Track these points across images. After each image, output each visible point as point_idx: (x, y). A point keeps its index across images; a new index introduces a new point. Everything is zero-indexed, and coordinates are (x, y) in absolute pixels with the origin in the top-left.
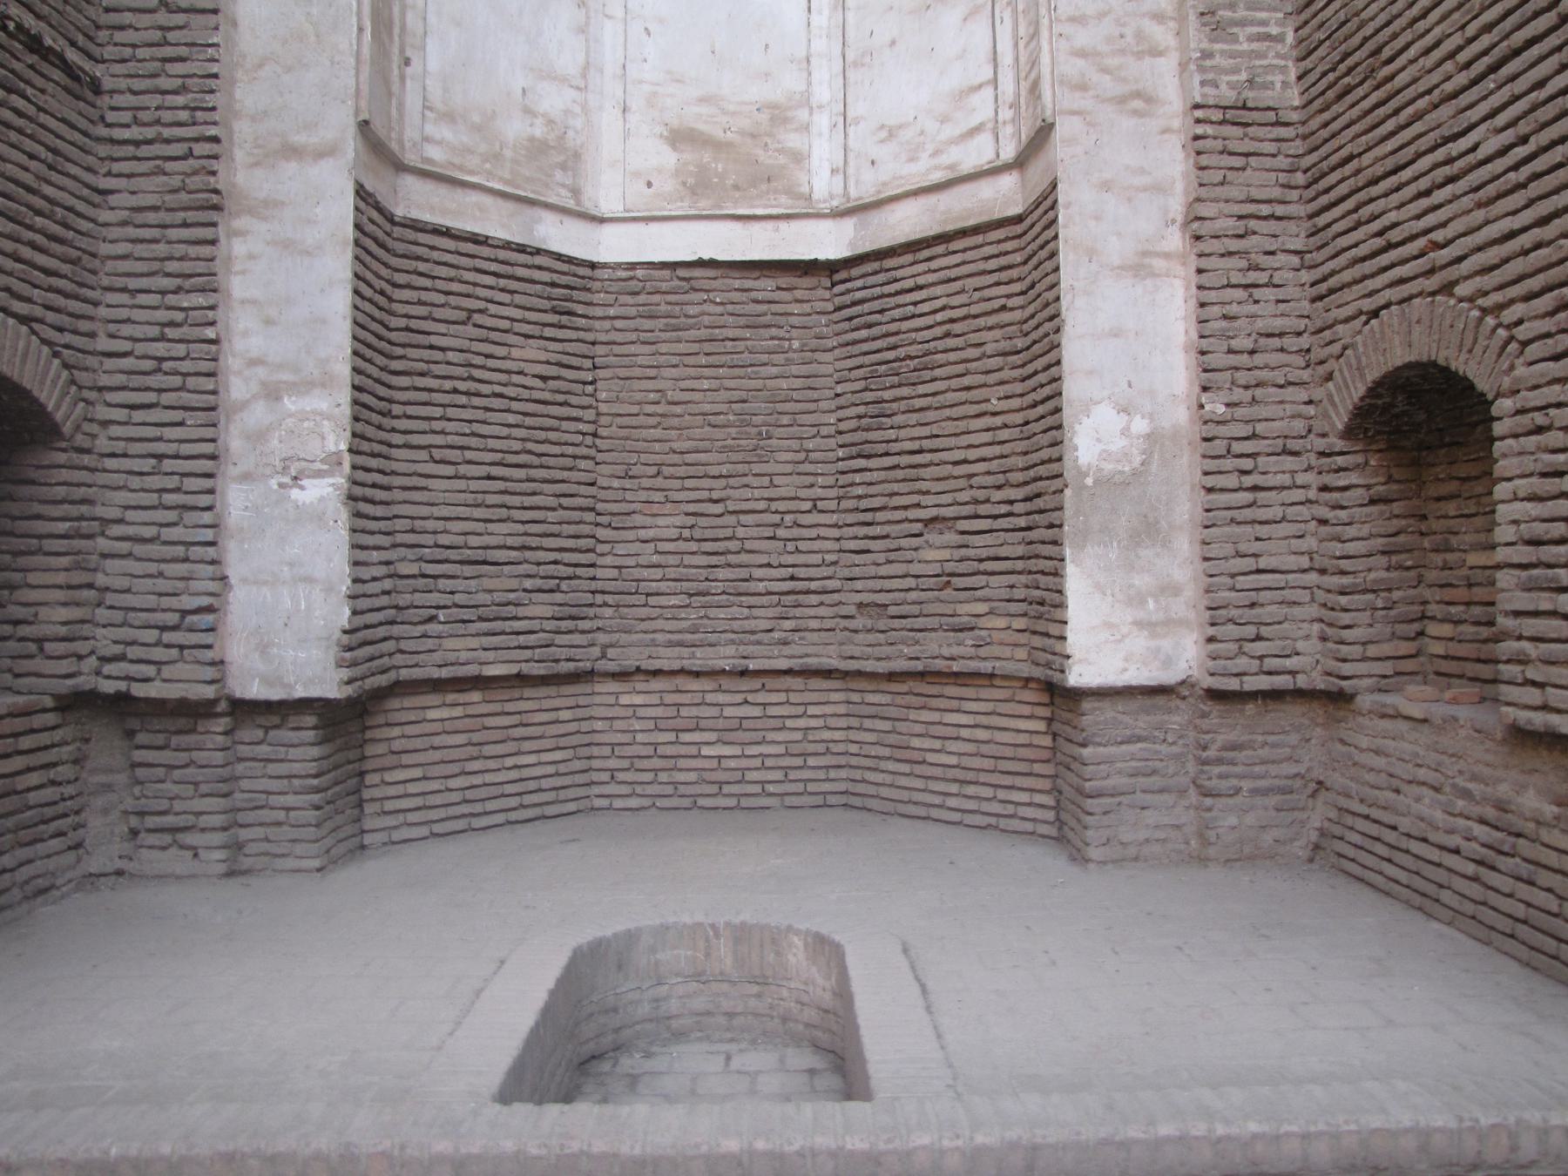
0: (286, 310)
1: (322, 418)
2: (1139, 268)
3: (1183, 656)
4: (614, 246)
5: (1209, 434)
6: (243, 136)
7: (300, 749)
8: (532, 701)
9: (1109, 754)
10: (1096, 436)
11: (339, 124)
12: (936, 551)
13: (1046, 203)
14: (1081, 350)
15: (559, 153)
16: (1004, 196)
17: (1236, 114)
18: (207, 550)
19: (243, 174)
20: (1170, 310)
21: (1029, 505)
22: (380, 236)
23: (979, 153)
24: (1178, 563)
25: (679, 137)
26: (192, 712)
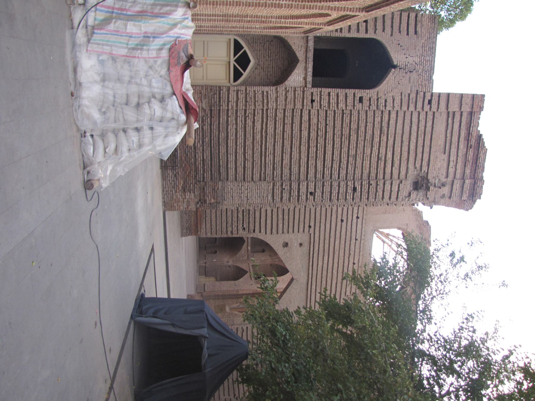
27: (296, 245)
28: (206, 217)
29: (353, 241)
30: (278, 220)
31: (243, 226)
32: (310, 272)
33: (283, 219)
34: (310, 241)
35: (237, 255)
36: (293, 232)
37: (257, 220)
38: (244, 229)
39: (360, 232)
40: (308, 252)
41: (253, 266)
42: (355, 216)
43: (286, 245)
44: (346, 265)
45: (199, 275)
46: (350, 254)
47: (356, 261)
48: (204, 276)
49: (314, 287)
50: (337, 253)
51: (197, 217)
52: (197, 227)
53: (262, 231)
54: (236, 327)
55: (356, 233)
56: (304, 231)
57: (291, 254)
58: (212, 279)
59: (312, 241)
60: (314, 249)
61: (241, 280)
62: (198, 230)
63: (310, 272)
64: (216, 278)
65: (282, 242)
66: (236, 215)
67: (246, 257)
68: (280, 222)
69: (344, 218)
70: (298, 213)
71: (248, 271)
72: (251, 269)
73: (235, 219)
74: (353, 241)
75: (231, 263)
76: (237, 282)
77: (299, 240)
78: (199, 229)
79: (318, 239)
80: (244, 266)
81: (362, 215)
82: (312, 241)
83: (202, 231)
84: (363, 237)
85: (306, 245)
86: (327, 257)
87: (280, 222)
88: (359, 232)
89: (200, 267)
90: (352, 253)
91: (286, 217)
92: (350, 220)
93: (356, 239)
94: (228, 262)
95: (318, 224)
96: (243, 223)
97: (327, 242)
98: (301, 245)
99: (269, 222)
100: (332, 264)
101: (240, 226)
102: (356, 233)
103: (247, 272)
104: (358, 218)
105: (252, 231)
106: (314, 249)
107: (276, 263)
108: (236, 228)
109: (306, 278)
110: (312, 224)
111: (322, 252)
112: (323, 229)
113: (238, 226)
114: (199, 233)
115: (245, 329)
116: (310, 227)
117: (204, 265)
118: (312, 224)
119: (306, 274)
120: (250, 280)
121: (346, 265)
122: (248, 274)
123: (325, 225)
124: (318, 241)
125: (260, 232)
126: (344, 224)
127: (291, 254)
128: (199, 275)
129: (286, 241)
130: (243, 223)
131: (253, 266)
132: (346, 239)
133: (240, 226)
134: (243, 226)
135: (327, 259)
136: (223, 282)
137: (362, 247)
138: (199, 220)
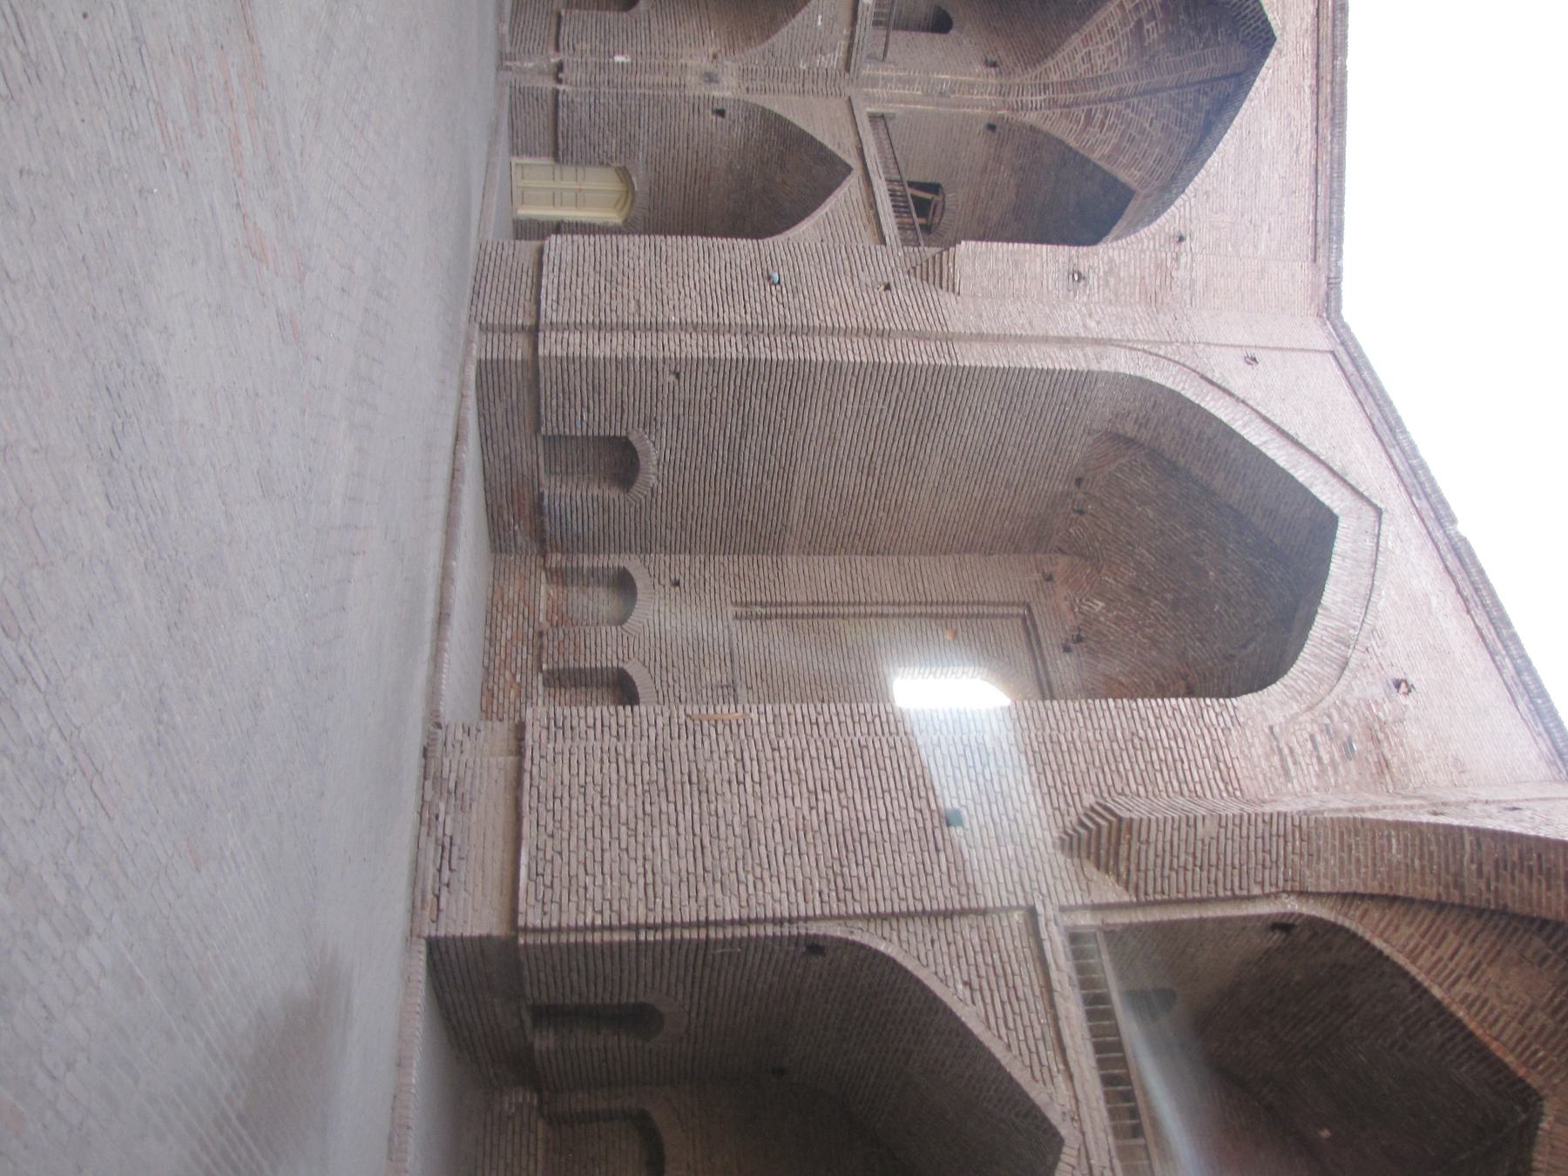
35: (781, 39)
41: (873, 118)
45: (515, 150)
48: (547, 161)
58: (602, 182)
61: (805, 231)
64: (624, 175)
67: (834, 59)
71: (853, 161)
72: (871, 151)
75: (728, 89)
76: (775, 245)
80: (821, 121)
89: (520, 99)
94: (710, 78)
103: (849, 169)
107: (1031, 118)
117: (549, 84)
120: (868, 238)
122: (850, 188)
128: (515, 150)
131: (873, 118)
136: (672, 244)
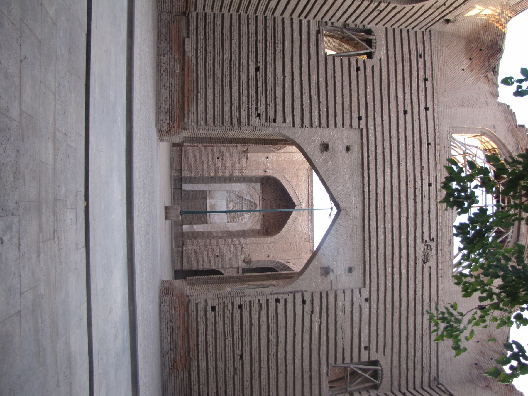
0: (201, 187)
1: (196, 189)
2: (203, 229)
3: (184, 231)
4: (208, 201)
5: (194, 232)
6: (210, 184)
7: (179, 187)
8: (180, 197)
9: (179, 227)
10: (195, 226)
11: (210, 189)
12: (189, 220)
13: (207, 223)
14: (199, 225)
15: (213, 198)
16: (209, 222)
17: (211, 233)
18: (189, 183)
19: (208, 184)
20: (201, 230)
21: (192, 223)
22: (205, 191)
23: (211, 221)
24: (189, 231)
25: (214, 204)
26: (181, 182)
27: (341, 148)
28: (197, 92)
29: (425, 146)
30: (311, 105)
31: (257, 109)
32: (366, 195)
33: (319, 102)
34: (362, 143)
36: (336, 126)
37: (279, 101)
38: (259, 115)
39: (433, 132)
40: (360, 162)
42: (423, 106)
43: (325, 147)
44: (418, 186)
46: (422, 167)
47: (432, 180)
49: (373, 223)
50: (403, 164)
51: (183, 94)
52: (182, 109)
53: (288, 120)
54: (248, 299)
55: (427, 133)
56: (351, 125)
57: (334, 164)
59: (365, 142)
60: (368, 157)
62: (184, 114)
63: (366, 195)
65: (318, 141)
66: (245, 92)
68: (315, 106)
69: (408, 108)
70: (340, 94)
73: (245, 99)
74: (425, 146)
77: (345, 141)
78: (186, 112)
79: (373, 139)
81: (432, 105)
82: (365, 142)
83: (191, 116)
84: (437, 141)
85: (356, 148)
86: (389, 171)
87: (315, 106)
88: (431, 131)
90: (425, 165)
91: (323, 100)
92: (416, 111)
93: (429, 144)
95: (371, 114)
96: (257, 105)
97: (387, 144)
98: (348, 149)
99: (297, 105)
100: (397, 183)
101: (253, 111)
102: (427, 133)
104: (427, 109)
105: (272, 120)
106: (368, 157)
108: (245, 114)
109: (360, 206)
110: (363, 114)
111: (382, 163)
112: (380, 123)
113: (248, 108)
114: (186, 120)
115: (264, 305)
116: (360, 118)
118: (363, 114)
119: (360, 200)
121: (418, 186)
123: (382, 117)
124: (373, 143)
125: (284, 121)
126: (409, 116)
127: (334, 164)
129: (326, 140)
130: (257, 105)
132: (413, 141)
133: (253, 111)
134: (257, 109)
135: (389, 174)
137: (438, 157)
138: (186, 98)
